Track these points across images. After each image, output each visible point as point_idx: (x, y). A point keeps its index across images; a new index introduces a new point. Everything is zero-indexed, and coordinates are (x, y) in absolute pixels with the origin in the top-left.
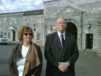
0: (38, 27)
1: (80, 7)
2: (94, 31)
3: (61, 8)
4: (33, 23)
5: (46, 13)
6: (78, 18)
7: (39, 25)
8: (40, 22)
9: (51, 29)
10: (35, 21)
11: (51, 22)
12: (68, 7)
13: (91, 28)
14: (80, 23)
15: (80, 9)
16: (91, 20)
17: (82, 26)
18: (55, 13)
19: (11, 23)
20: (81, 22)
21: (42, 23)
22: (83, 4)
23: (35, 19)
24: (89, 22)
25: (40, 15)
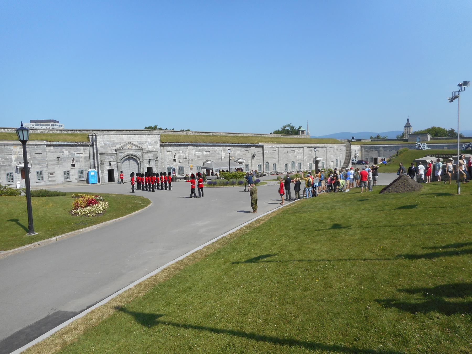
1: (140, 144)
2: (153, 165)
3: (120, 142)
4: (70, 156)
6: (139, 154)
7: (81, 159)
8: (81, 155)
9: (110, 164)
10: (72, 154)
11: (109, 157)
12: (130, 143)
15: (140, 146)
16: (150, 156)
19: (14, 157)
20: (142, 157)
21: (85, 157)
23: (72, 152)
24: (149, 157)
25: (82, 148)
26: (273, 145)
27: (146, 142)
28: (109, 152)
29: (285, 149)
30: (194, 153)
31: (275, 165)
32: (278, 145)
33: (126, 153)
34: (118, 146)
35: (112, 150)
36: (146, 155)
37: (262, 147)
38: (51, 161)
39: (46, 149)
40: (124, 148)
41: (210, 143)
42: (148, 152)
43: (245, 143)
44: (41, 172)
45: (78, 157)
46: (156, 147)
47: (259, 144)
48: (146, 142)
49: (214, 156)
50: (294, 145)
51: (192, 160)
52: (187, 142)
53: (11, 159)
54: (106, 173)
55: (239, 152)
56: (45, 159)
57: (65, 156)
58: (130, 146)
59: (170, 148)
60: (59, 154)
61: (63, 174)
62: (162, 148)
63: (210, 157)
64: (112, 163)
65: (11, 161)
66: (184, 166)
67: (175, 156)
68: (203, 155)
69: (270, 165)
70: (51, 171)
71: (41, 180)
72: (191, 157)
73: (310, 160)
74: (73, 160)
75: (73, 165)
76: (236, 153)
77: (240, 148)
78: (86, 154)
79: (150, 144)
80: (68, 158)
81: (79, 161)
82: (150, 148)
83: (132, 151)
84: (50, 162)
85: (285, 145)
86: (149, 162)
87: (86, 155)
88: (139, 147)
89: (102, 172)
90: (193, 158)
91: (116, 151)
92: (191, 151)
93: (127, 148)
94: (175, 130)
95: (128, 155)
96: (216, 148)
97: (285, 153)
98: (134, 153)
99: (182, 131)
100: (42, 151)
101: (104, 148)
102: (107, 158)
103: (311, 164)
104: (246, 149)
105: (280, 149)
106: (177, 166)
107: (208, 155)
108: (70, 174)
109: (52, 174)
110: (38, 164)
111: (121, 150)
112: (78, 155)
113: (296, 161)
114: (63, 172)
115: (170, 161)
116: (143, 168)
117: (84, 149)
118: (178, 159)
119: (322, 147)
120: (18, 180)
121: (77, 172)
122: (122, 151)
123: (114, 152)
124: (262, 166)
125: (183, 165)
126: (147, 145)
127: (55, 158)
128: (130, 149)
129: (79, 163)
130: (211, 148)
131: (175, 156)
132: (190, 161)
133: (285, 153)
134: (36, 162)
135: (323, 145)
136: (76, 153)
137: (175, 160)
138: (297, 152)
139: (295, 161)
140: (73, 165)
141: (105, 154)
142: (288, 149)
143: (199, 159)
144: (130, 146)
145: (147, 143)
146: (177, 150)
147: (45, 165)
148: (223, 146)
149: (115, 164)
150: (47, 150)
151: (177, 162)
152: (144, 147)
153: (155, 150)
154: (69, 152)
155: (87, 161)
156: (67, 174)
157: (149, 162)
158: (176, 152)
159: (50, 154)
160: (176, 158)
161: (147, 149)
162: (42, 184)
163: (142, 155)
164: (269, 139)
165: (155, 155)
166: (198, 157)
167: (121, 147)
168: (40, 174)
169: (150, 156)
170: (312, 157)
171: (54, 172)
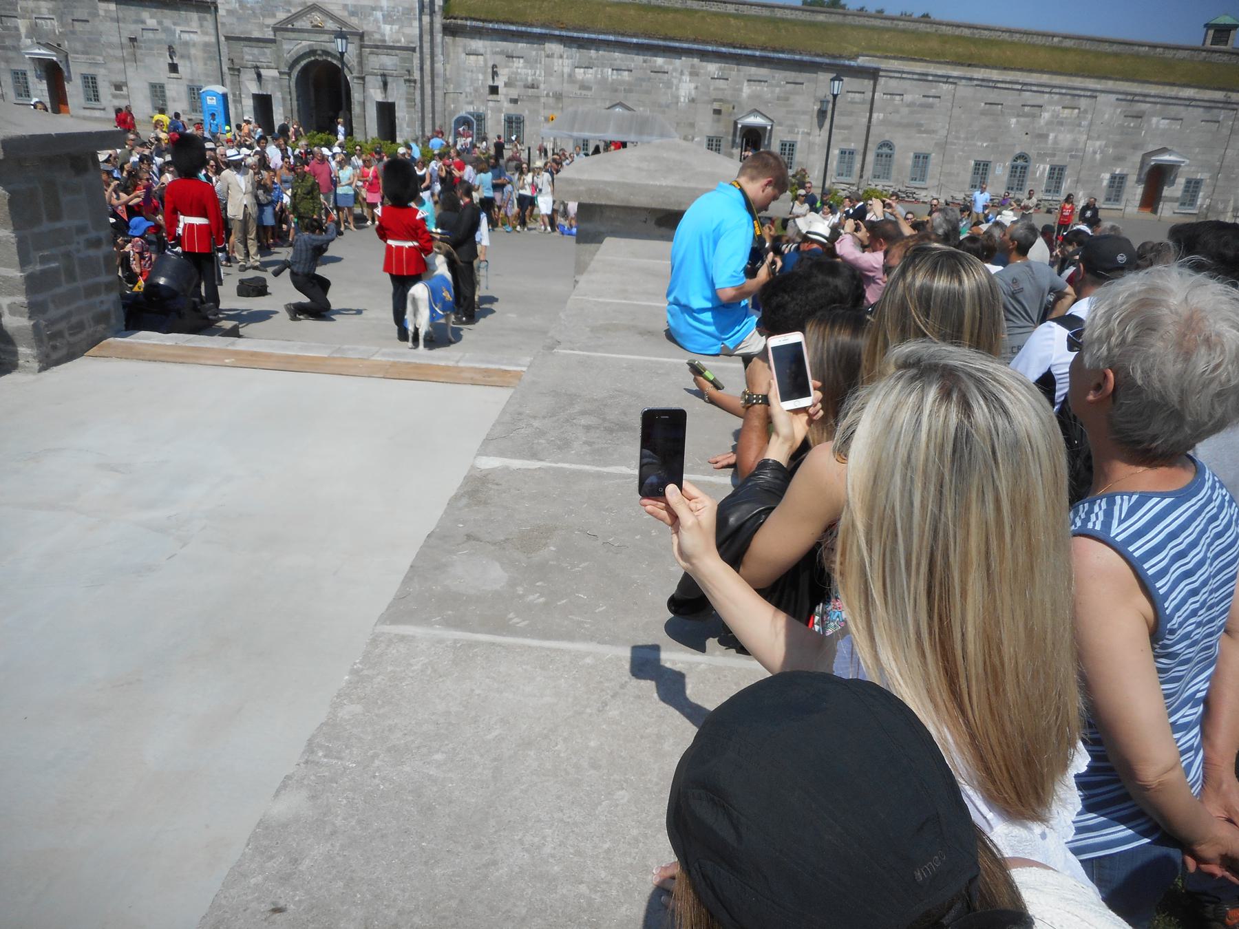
0: (187, 57)
1: (353, 14)
2: (397, 95)
4: (161, 36)
5: (230, 12)
7: (193, 51)
9: (259, 76)
10: (166, 30)
11: (256, 51)
12: (314, 8)
13: (389, 86)
14: (357, 68)
15: (354, 21)
16: (388, 61)
17: (363, 79)
18: (271, 21)
20: (361, 63)
21: (206, 45)
22: (363, 7)
23: (167, 23)
24: (383, 67)
26: (933, 69)
27: (374, 9)
28: (256, 34)
29: (993, 96)
30: (567, 70)
31: (921, 159)
32: (956, 72)
33: (304, 45)
34: (281, 16)
35: (262, 26)
36: (373, 58)
37: (873, 74)
38: (111, 45)
39: (96, 9)
40: (298, 25)
41: (635, 36)
42: (383, 47)
43: (792, 51)
44: (94, 78)
45: (186, 44)
46: (407, 30)
47: (862, 61)
48: (374, 9)
49: (648, 92)
50: (1045, 78)
51: (558, 97)
52: (543, 26)
53: (17, 28)
54: (248, 103)
55: (757, 88)
56: (98, 41)
57: (150, 35)
58: (317, 18)
59: (477, 44)
60: (133, 27)
61: (147, 91)
62: (448, 39)
63: (630, 91)
64: (263, 72)
65: (19, 37)
66: (526, 113)
67: (495, 74)
68: (603, 82)
69: (896, 156)
70: (119, 78)
71: (94, 104)
72: (556, 85)
73: (1119, 159)
74: (172, 52)
75: (174, 68)
76: (747, 90)
77: (762, 72)
78: (206, 33)
79: (388, 18)
80: (159, 42)
81: (189, 57)
82: (389, 32)
83: (326, 37)
84: (111, 52)
85: (995, 75)
86: (385, 84)
87: (206, 39)
88: (344, 24)
89: (238, 101)
90: (567, 87)
91: (276, 30)
92: (557, 64)
93: (309, 26)
94: (886, 13)
95: (312, 52)
96: (660, 61)
97: (983, 113)
98: (330, 47)
99: (905, 17)
100: (89, 14)
101: (239, 19)
102: (249, 54)
103: (1118, 183)
104: (791, 75)
105: (964, 90)
106: (500, 111)
107: (622, 82)
108: (168, 93)
109: (118, 87)
110: (83, 53)
111: (287, 30)
112: (185, 37)
113: (1042, 157)
114: (147, 85)
115: (476, 90)
116: (363, 104)
117: (200, 19)
118: (506, 85)
119: (1211, 105)
120: (39, 93)
121: (183, 90)
122: (292, 35)
123: (269, 34)
124: (858, 159)
125: (523, 110)
126: (376, 21)
127: (125, 41)
128: (318, 30)
129: (188, 63)
130: (637, 60)
131: (495, 74)
132: (551, 101)
133: (983, 113)
134: (79, 46)
135: (1219, 95)
136: (178, 29)
137: (494, 90)
138: (1055, 115)
139: (1032, 153)
140: (174, 68)
141: (239, 39)
142: (1010, 98)
143: (585, 98)
144: (317, 18)
145: (379, 14)
146: (501, 53)
147: (100, 59)
148: (689, 53)
149: (274, 79)
150: (102, 13)
151: (500, 97)
152: (365, 28)
153: (403, 42)
154: (160, 23)
155: (211, 58)
156: (158, 91)
157: (385, 84)
158: (499, 59)
159: (108, 24)
160: (500, 82)
161: (377, 36)
162: (97, 114)
163: (360, 56)
164: (935, 44)
165: (404, 60)
166: (584, 86)
167: (290, 20)
168: (90, 83)
169: (388, 61)
170: (1135, 147)
171: (125, 84)
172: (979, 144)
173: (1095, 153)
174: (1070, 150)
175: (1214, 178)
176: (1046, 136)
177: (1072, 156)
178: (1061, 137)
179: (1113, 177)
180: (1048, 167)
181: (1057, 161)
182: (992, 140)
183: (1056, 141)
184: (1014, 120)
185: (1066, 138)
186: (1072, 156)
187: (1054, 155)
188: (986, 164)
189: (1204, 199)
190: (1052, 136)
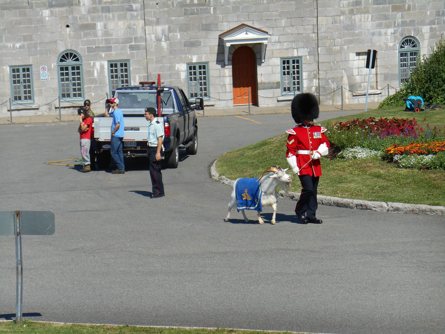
139: (80, 49)
170: (207, 28)
172: (10, 45)
173: (159, 40)
174: (128, 40)
175: (315, 53)
176: (93, 27)
177: (131, 48)
178: (111, 26)
179: (192, 67)
180: (106, 64)
181: (117, 55)
182: (25, 38)
183: (106, 33)
184: (46, 12)
185: (118, 27)
186: (131, 48)
187: (109, 49)
188: (27, 69)
189: (310, 80)
190: (99, 26)
